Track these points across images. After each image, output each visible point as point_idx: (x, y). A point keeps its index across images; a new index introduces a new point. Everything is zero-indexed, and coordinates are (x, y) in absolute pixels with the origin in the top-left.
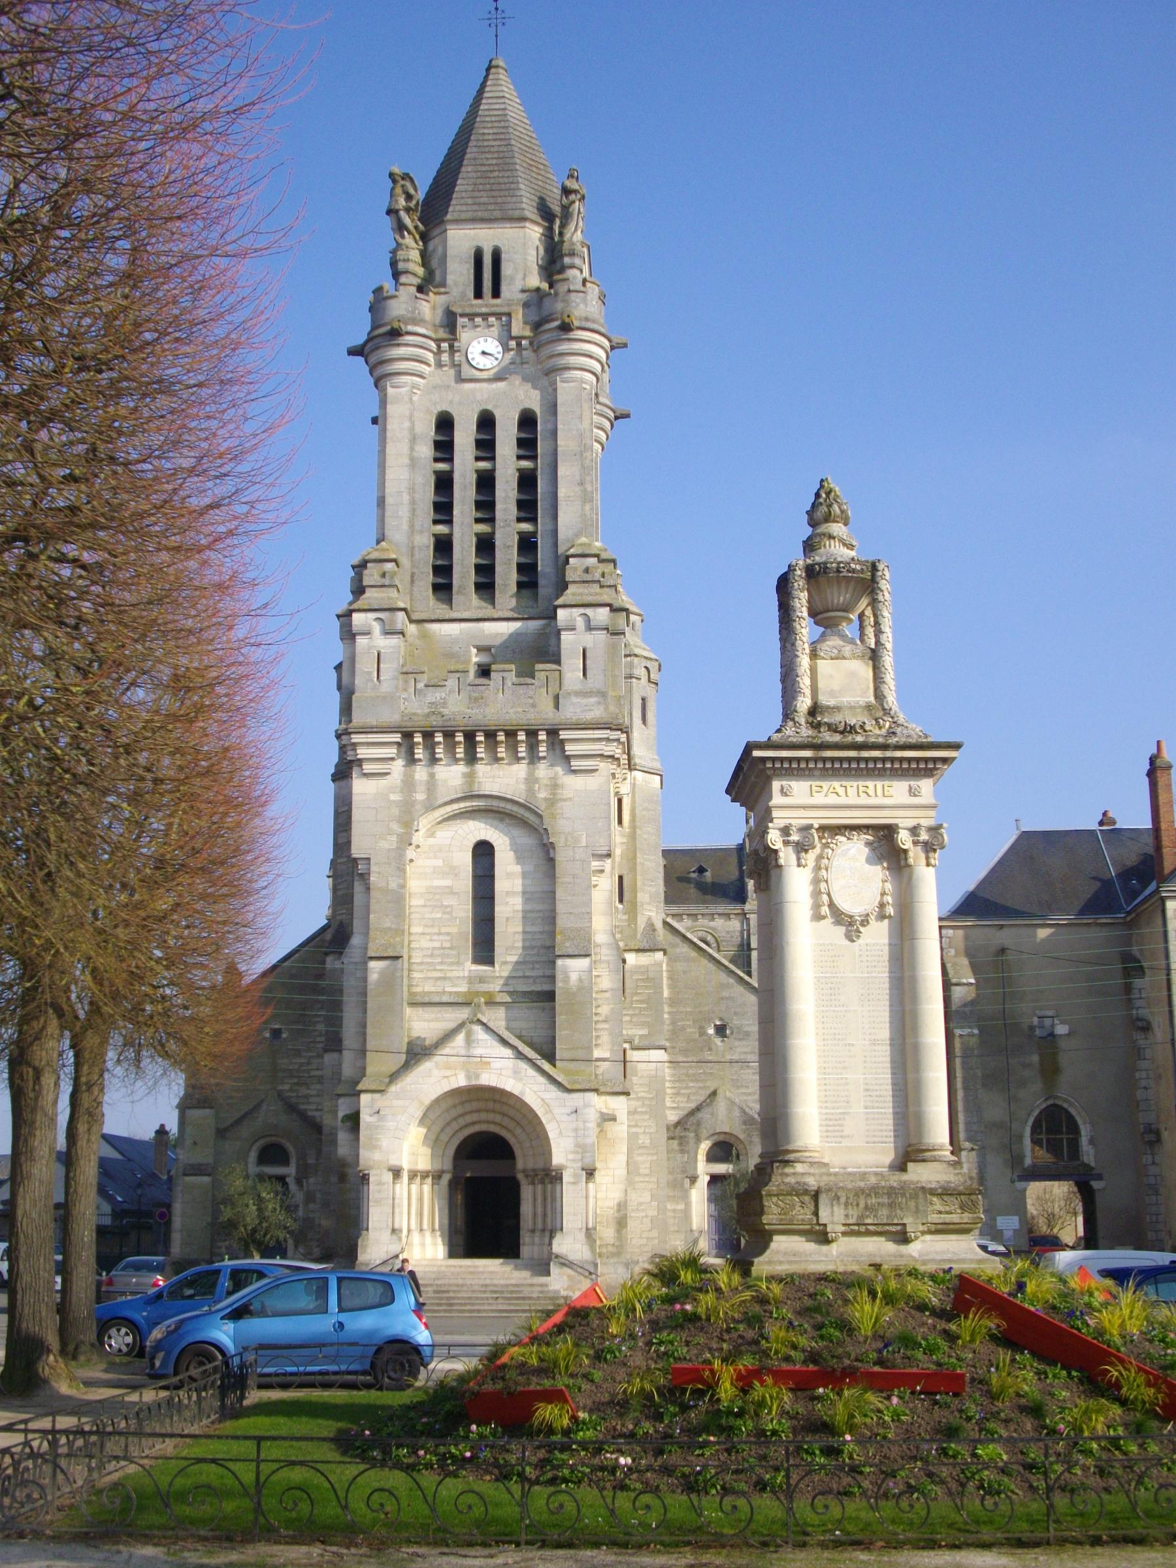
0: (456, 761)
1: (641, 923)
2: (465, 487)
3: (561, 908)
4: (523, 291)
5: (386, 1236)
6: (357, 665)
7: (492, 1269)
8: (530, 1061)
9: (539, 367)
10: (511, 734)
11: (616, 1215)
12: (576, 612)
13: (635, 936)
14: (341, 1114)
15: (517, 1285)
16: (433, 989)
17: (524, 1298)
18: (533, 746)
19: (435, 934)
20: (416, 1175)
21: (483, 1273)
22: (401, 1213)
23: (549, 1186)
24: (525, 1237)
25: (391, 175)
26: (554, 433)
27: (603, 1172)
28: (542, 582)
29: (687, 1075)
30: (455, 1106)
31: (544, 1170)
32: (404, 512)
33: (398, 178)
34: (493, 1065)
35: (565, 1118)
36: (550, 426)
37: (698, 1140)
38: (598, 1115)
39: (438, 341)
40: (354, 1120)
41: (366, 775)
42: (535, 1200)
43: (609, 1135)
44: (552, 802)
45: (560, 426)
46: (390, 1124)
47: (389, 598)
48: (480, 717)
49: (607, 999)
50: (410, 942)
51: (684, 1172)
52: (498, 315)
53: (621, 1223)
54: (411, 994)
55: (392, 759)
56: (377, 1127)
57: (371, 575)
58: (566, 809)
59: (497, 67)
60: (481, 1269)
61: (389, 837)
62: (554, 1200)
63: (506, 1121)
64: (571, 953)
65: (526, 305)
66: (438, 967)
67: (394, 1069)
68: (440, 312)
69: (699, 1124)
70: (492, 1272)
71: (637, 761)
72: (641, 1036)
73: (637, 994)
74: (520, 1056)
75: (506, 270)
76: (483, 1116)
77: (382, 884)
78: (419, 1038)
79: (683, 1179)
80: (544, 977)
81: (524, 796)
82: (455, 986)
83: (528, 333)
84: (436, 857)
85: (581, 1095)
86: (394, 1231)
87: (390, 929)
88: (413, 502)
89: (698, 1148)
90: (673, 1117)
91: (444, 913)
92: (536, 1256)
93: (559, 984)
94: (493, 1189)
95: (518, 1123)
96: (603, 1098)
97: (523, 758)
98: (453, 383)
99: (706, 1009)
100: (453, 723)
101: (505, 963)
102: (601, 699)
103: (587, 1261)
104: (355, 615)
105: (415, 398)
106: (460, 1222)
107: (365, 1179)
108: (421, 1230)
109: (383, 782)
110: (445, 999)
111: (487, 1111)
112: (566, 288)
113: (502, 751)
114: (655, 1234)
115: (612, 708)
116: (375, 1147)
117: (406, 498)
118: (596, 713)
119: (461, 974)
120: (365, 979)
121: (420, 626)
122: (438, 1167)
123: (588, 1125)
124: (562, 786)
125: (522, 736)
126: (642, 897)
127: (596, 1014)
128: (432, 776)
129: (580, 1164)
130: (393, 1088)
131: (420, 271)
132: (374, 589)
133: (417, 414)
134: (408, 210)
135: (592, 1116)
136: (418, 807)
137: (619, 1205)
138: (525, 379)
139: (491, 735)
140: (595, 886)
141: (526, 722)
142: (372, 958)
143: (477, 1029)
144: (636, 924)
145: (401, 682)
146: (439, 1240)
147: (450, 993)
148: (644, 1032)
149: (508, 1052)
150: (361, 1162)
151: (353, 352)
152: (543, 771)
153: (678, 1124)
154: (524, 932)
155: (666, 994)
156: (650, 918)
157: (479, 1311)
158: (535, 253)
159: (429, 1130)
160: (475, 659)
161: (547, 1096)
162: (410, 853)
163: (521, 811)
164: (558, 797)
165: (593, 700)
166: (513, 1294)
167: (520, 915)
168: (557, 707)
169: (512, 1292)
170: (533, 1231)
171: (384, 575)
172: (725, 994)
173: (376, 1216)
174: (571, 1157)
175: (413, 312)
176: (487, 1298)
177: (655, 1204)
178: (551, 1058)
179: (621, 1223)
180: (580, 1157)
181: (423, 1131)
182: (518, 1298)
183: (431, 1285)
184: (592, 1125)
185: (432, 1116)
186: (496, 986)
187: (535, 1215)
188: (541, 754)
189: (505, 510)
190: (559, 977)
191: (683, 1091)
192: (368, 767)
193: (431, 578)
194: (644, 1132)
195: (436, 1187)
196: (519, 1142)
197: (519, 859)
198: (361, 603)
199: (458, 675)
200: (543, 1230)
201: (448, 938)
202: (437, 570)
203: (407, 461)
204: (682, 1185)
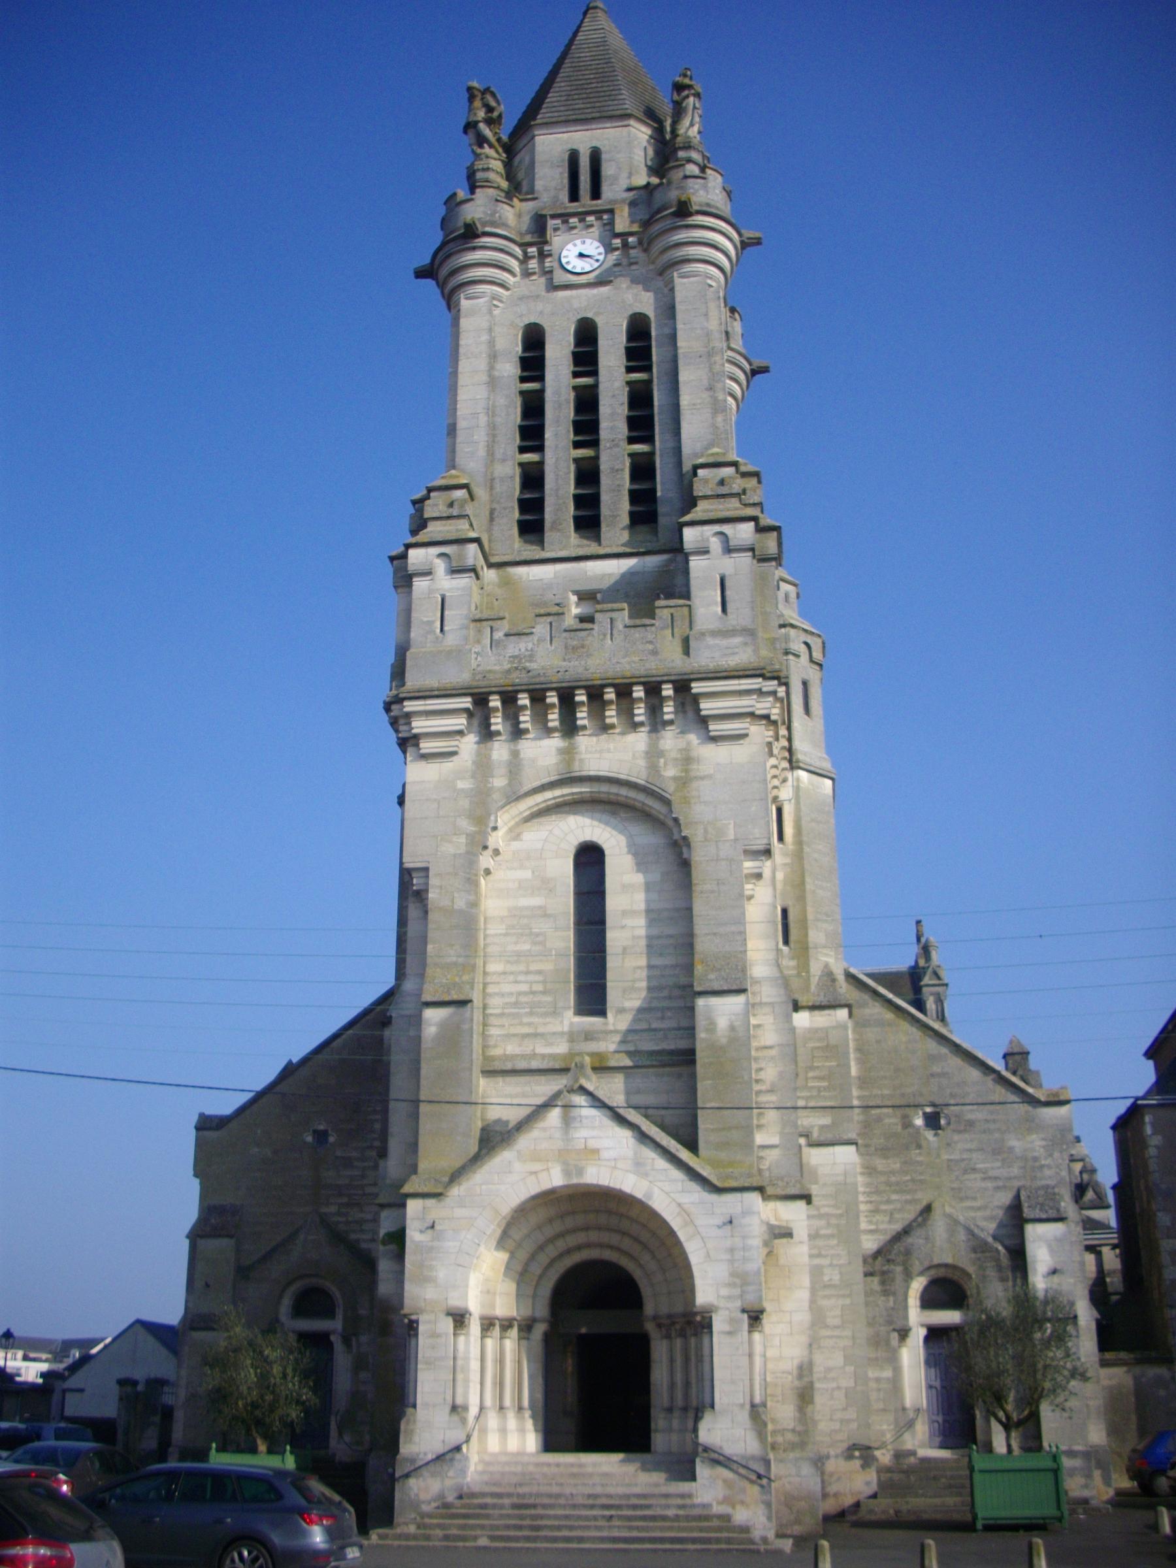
0: (549, 731)
1: (816, 969)
2: (560, 406)
3: (700, 928)
4: (630, 189)
5: (442, 1416)
6: (414, 615)
7: (605, 1469)
9: (651, 267)
10: (624, 692)
11: (797, 1383)
12: (709, 530)
13: (807, 988)
14: (382, 1232)
15: (644, 1496)
17: (653, 1518)
18: (654, 710)
19: (521, 973)
21: (591, 1475)
22: (467, 1381)
23: (693, 1340)
24: (659, 1421)
25: (470, 89)
26: (673, 338)
27: (774, 1318)
28: (662, 509)
30: (551, 1221)
31: (684, 1315)
32: (481, 436)
33: (476, 93)
34: (605, 1155)
36: (667, 331)
37: (908, 1276)
38: (764, 1228)
39: (524, 246)
40: (398, 1238)
41: (425, 757)
42: (672, 1361)
43: (782, 1261)
44: (684, 781)
45: (679, 326)
46: (451, 1245)
47: (457, 530)
48: (580, 670)
49: (772, 1058)
50: (485, 985)
52: (598, 213)
53: (805, 1396)
54: (487, 1058)
55: (460, 733)
56: (431, 1249)
57: (436, 506)
58: (704, 790)
59: (595, 8)
60: (590, 1470)
61: (455, 839)
62: (700, 1359)
63: (626, 1244)
64: (716, 987)
65: (633, 204)
66: (525, 1020)
67: (458, 1164)
68: (527, 219)
69: (908, 1253)
70: (606, 1475)
71: (800, 756)
72: (822, 1127)
73: (812, 1068)
74: (643, 1137)
75: (607, 170)
76: (594, 1236)
77: (445, 903)
78: (498, 1121)
79: (888, 1333)
80: (679, 1029)
81: (644, 775)
82: (552, 1044)
83: (635, 228)
84: (522, 867)
85: (737, 1196)
86: (454, 1408)
87: (455, 964)
88: (492, 428)
89: (908, 1288)
90: (870, 1244)
91: (534, 943)
92: (674, 1449)
93: (701, 1035)
94: (612, 1344)
96: (772, 1205)
97: (642, 724)
98: (543, 293)
99: (909, 1090)
100: (542, 679)
101: (621, 1011)
102: (748, 639)
103: (753, 1458)
104: (412, 553)
105: (496, 312)
108: (501, 1408)
109: (448, 766)
110: (535, 1065)
111: (599, 1228)
112: (681, 175)
113: (611, 715)
114: (852, 1414)
115: (764, 652)
116: (425, 1280)
117: (483, 420)
118: (743, 656)
119: (559, 1029)
120: (418, 1039)
121: (501, 571)
122: (527, 1312)
123: (750, 1242)
124: (698, 760)
125: (639, 692)
126: (816, 936)
127: (757, 1081)
128: (515, 754)
129: (738, 1304)
130: (455, 1191)
131: (505, 184)
132: (439, 523)
133: (497, 330)
134: (489, 122)
136: (496, 796)
137: (801, 1368)
138: (635, 281)
139: (595, 694)
140: (750, 898)
141: (643, 672)
142: (428, 1004)
143: (580, 1100)
144: (808, 972)
145: (472, 633)
146: (529, 1424)
147: (543, 1056)
148: (826, 1120)
151: (421, 274)
152: (670, 740)
153: (878, 1253)
154: (650, 967)
155: (854, 1071)
156: (827, 965)
157: (581, 1540)
158: (642, 154)
160: (575, 611)
161: (685, 1199)
162: (485, 860)
163: (641, 797)
164: (693, 774)
165: (737, 640)
166: (634, 1508)
167: (643, 942)
168: (687, 651)
169: (635, 1507)
170: (670, 1410)
171: (451, 505)
172: (936, 1069)
173: (428, 1385)
174: (724, 1292)
175: (493, 214)
176: (595, 1518)
178: (693, 1146)
179: (805, 1396)
180: (737, 1291)
181: (503, 1256)
182: (644, 1518)
183: (510, 1495)
184: (756, 1242)
185: (517, 1234)
186: (609, 1045)
187: (672, 1386)
188: (666, 717)
189: (612, 428)
190: (701, 1022)
191: (883, 1207)
192: (426, 746)
193: (516, 515)
194: (831, 1265)
195: (524, 1342)
197: (641, 865)
198: (422, 537)
199: (549, 619)
200: (685, 1409)
201: (540, 978)
202: (524, 506)
203: (484, 378)
204: (888, 1342)
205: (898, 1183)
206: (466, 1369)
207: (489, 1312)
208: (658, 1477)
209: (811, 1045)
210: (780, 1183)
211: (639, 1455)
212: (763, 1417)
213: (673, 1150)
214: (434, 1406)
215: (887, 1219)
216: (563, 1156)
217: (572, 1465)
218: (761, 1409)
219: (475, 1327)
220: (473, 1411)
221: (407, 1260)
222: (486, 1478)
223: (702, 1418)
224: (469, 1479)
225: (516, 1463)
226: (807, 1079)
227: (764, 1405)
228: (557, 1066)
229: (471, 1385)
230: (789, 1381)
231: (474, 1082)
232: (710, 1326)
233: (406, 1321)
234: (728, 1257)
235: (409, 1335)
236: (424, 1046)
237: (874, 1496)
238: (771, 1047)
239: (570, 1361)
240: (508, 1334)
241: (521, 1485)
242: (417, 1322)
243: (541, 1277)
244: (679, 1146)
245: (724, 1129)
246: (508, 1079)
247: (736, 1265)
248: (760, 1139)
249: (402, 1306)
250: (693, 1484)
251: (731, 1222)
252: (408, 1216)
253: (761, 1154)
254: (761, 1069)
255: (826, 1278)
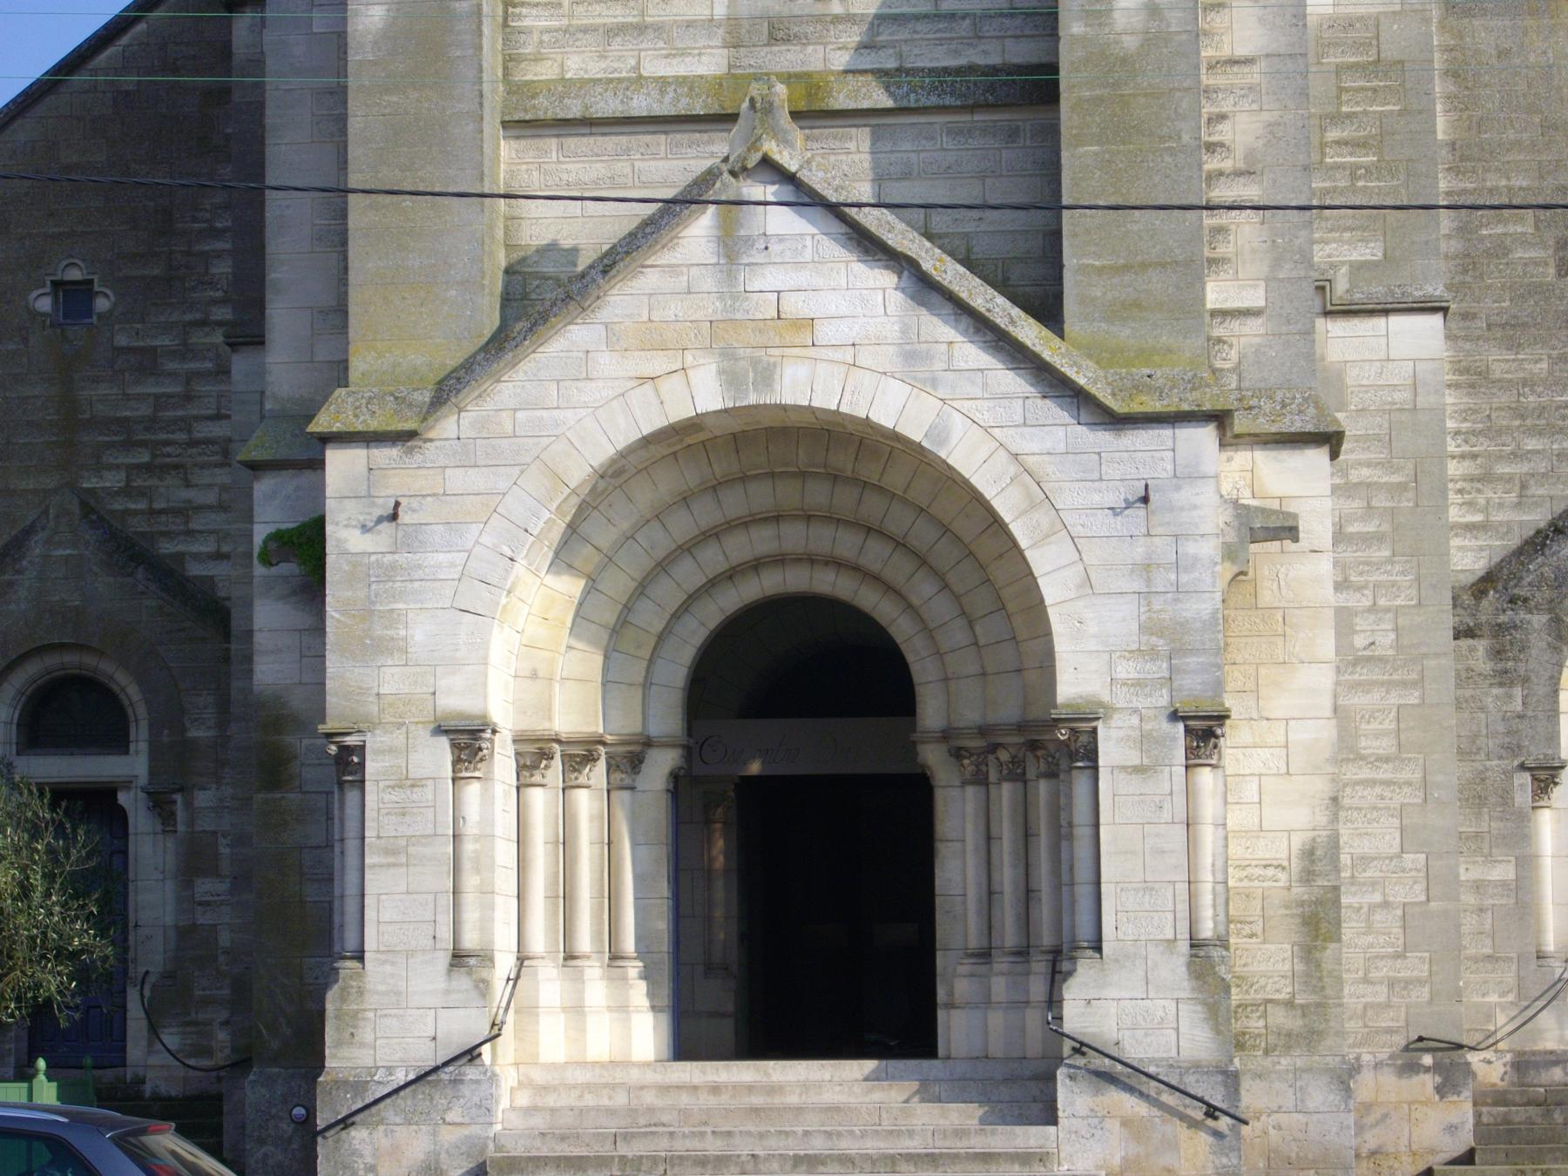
7: (831, 1097)
8: (961, 309)
11: (1299, 891)
14: (260, 533)
16: (596, 69)
20: (546, 755)
21: (799, 1110)
22: (487, 891)
24: (956, 980)
29: (1519, 412)
30: (685, 500)
31: (1021, 727)
34: (826, 332)
35: (1103, 523)
40: (306, 546)
43: (1267, 597)
46: (440, 560)
51: (1513, 749)
53: (1318, 923)
54: (517, 90)
56: (390, 572)
60: (793, 1099)
62: (1062, 833)
63: (875, 554)
67: (453, 360)
70: (835, 1109)
72: (1357, 268)
73: (1336, 118)
74: (925, 288)
76: (794, 537)
82: (683, 53)
85: (1166, 433)
86: (458, 958)
90: (1469, 559)
92: (997, 1048)
95: (922, 561)
96: (1242, 458)
103: (1196, 1067)
106: (724, 931)
107: (348, 764)
108: (570, 957)
110: (641, 105)
114: (1415, 966)
116: (378, 648)
120: (339, 40)
122: (629, 724)
123: (1190, 548)
127: (1211, 147)
129: (1162, 699)
130: (447, 427)
135: (1205, 516)
137: (1309, 854)
146: (639, 992)
147: (663, 83)
148: (1370, 251)
149: (881, 281)
150: (332, 701)
153: (1486, 583)
155: (1442, 127)
159: (592, 588)
161: (1030, 443)
170: (985, 955)
173: (392, 905)
174: (1127, 670)
177: (1414, 859)
178: (1047, 308)
179: (1318, 923)
181: (571, 587)
184: (1208, 549)
185: (604, 534)
187: (990, 894)
191: (1503, 469)
194: (1373, 609)
196: (928, 631)
200: (1022, 953)
204: (1506, 797)
205: (1542, 410)
206: (485, 864)
207: (540, 726)
208: (963, 1115)
209: (1332, 60)
210: (1267, 406)
211: (912, 1063)
212: (1222, 970)
213: (1001, 322)
214: (410, 954)
215: (1512, 497)
216: (719, 336)
217: (750, 1088)
218: (1216, 953)
219: (503, 762)
220: (505, 963)
221: (328, 599)
222: (539, 1122)
223: (1070, 973)
224: (498, 1127)
225: (613, 1087)
226: (1323, 145)
227: (1223, 942)
228: (699, 110)
229: (499, 900)
230: (1281, 885)
231: (487, 149)
232: (1092, 755)
233: (333, 749)
234: (1138, 585)
235: (341, 784)
236: (354, 57)
237: (1468, 1158)
238: (1248, 61)
239: (720, 844)
240: (582, 780)
241: (628, 1137)
242: (361, 749)
243: (661, 638)
244: (1016, 312)
245: (1126, 268)
246: (571, 142)
247: (1157, 604)
248: (1217, 294)
249: (321, 715)
250: (1052, 1129)
251: (1145, 500)
252: (330, 491)
253: (1218, 332)
254: (1222, 117)
255: (1360, 641)
